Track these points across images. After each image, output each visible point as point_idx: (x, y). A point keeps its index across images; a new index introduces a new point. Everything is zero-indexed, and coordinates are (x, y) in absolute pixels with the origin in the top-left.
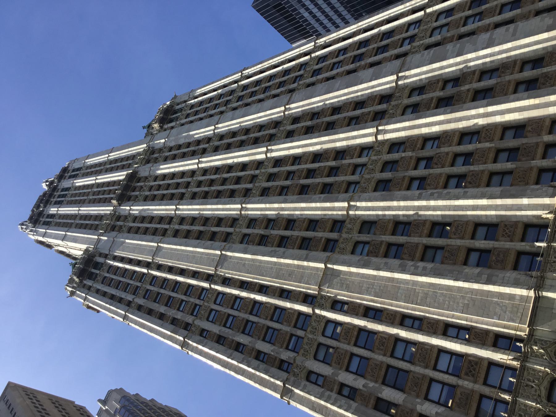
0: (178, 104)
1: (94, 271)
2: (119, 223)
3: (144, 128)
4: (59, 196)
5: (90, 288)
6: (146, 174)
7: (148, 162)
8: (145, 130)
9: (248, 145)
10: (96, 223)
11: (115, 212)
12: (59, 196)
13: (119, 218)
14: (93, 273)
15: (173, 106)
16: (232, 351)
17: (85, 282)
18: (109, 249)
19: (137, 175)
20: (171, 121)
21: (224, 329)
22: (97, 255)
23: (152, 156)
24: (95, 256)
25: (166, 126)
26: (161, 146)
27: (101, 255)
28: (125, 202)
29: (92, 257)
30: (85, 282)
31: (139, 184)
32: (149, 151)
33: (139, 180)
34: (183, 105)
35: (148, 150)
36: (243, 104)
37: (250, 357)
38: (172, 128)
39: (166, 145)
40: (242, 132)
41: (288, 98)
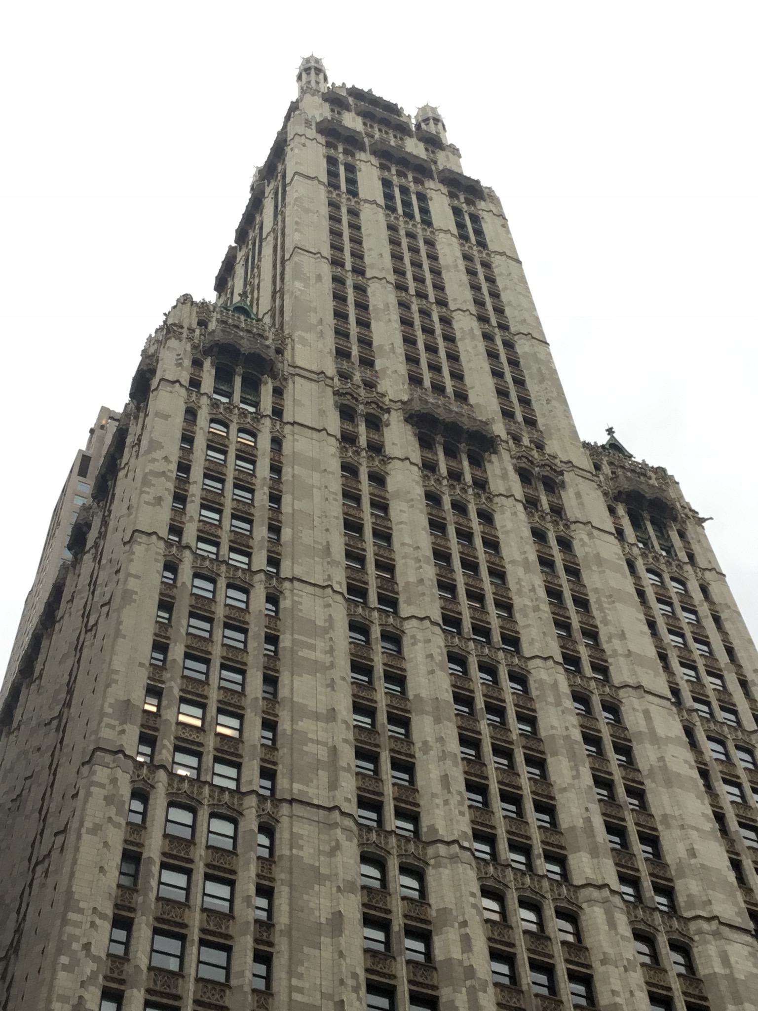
0: (682, 535)
1: (238, 381)
2: (362, 429)
3: (610, 431)
4: (404, 190)
5: (195, 383)
6: (496, 485)
7: (525, 476)
8: (602, 439)
9: (604, 814)
10: (355, 351)
11: (388, 411)
12: (404, 190)
13: (375, 424)
14: (230, 382)
15: (675, 519)
16: (111, 915)
17: (207, 364)
18: (297, 420)
19: (487, 454)
20: (637, 523)
21: (156, 869)
22: (278, 384)
23: (541, 487)
24: (274, 377)
25: (621, 510)
26: (572, 509)
27: (278, 392)
28: (415, 435)
29: (272, 370)
30: (207, 364)
31: (466, 463)
32: (552, 475)
33: (476, 462)
34: (683, 556)
35: (555, 471)
36: (706, 764)
37: (105, 978)
38: (620, 534)
39: (573, 527)
40: (634, 781)
41: (738, 921)
